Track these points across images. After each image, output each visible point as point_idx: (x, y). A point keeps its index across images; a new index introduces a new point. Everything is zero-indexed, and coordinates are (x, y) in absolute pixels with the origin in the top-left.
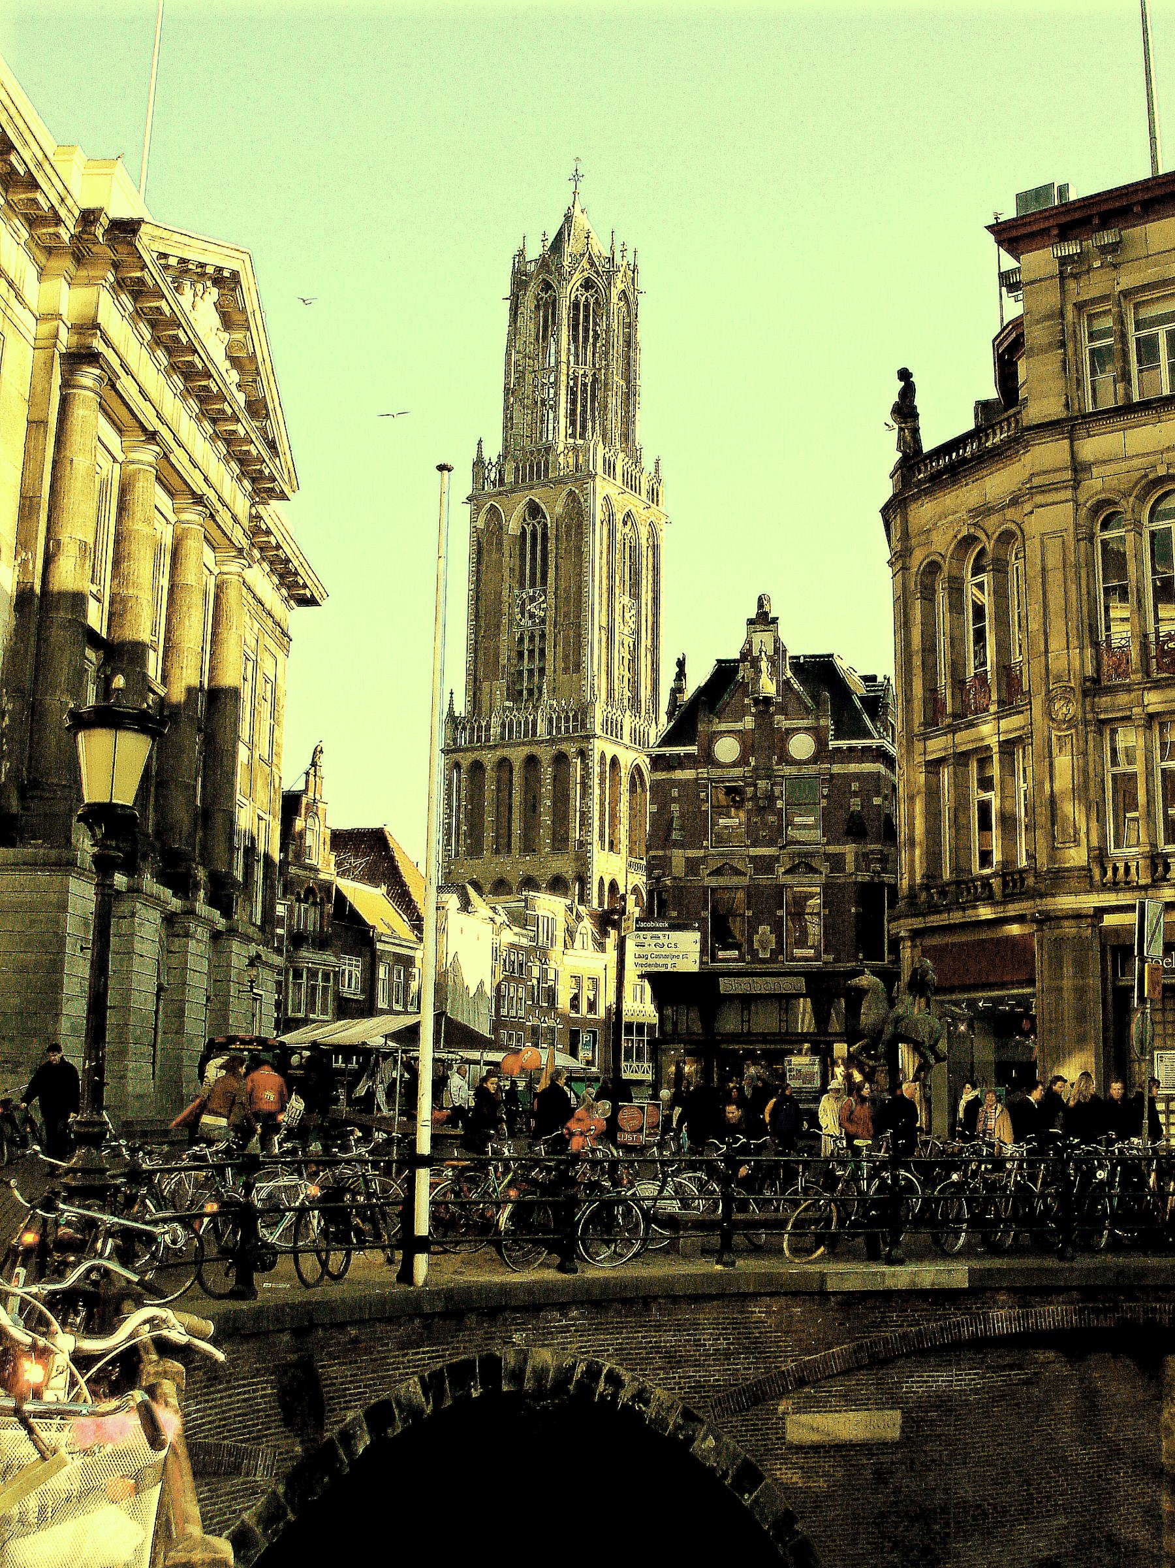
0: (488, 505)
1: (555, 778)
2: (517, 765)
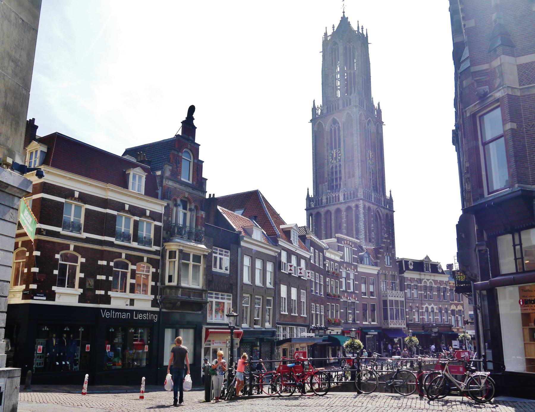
0: (318, 122)
1: (347, 216)
2: (333, 212)
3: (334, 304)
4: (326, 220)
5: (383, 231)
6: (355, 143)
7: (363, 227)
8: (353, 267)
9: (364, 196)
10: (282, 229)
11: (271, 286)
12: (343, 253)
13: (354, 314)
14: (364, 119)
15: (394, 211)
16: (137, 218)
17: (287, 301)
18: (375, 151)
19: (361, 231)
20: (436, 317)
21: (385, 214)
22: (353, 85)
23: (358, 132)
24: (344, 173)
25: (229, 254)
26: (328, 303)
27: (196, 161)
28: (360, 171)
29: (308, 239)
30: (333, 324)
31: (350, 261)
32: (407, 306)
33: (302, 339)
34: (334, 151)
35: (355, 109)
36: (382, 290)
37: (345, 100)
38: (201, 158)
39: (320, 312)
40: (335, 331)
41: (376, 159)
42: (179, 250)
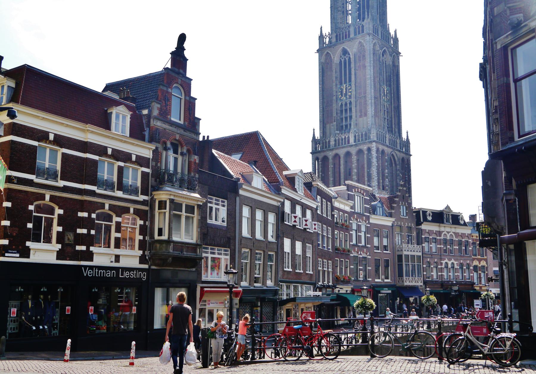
0: (326, 53)
2: (342, 156)
3: (343, 260)
4: (334, 165)
5: (398, 177)
6: (368, 77)
7: (376, 173)
8: (364, 218)
9: (377, 138)
10: (286, 176)
11: (273, 240)
12: (353, 202)
13: (365, 270)
14: (379, 49)
15: (411, 155)
16: (122, 164)
17: (291, 256)
18: (390, 86)
19: (374, 177)
20: (456, 274)
21: (401, 158)
22: (366, 9)
23: (372, 65)
24: (355, 111)
25: (226, 204)
26: (336, 259)
27: (188, 98)
28: (373, 109)
29: (314, 187)
30: (342, 281)
31: (362, 211)
32: (425, 261)
33: (308, 299)
34: (343, 86)
35: (368, 38)
36: (397, 244)
37: (357, 27)
38: (193, 95)
39: (328, 268)
40: (344, 289)
41: (391, 95)
42: (170, 199)
